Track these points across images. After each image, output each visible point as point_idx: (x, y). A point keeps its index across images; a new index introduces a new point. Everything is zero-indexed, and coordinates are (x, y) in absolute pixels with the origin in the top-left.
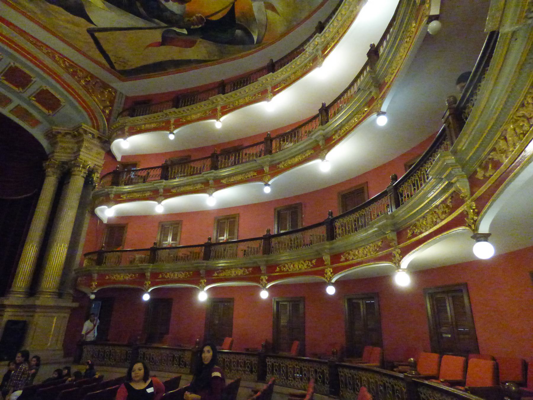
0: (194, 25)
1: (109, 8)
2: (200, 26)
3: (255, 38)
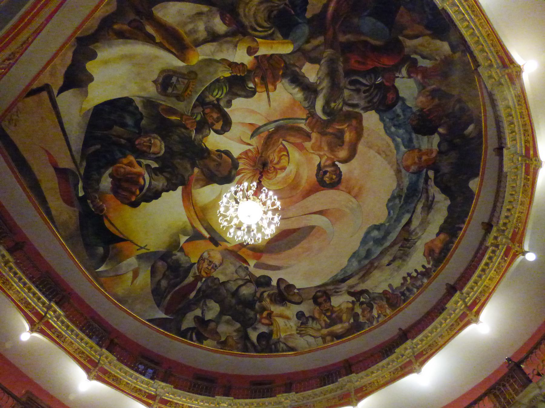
0: (92, 202)
1: (85, 114)
2: (93, 210)
3: (100, 269)
